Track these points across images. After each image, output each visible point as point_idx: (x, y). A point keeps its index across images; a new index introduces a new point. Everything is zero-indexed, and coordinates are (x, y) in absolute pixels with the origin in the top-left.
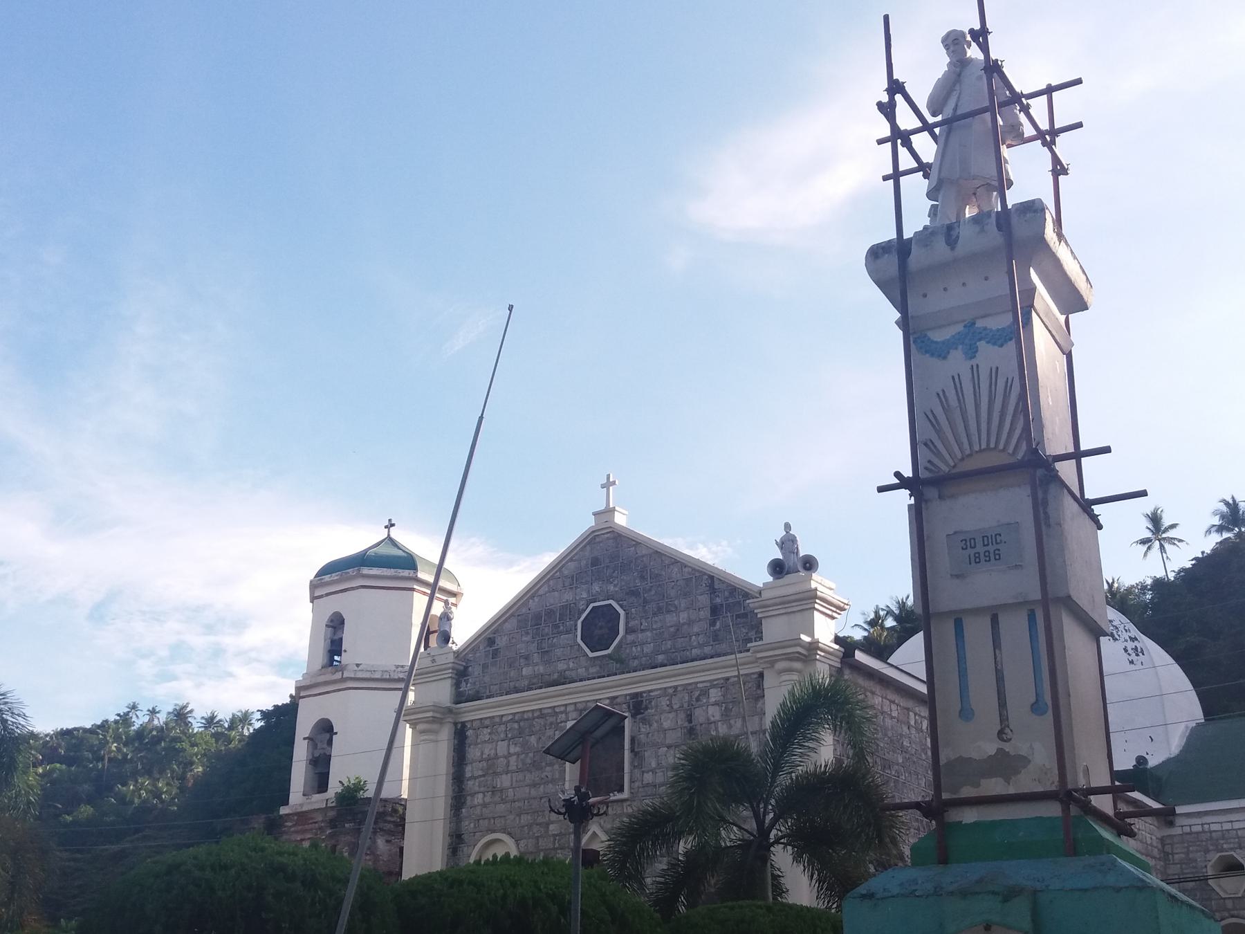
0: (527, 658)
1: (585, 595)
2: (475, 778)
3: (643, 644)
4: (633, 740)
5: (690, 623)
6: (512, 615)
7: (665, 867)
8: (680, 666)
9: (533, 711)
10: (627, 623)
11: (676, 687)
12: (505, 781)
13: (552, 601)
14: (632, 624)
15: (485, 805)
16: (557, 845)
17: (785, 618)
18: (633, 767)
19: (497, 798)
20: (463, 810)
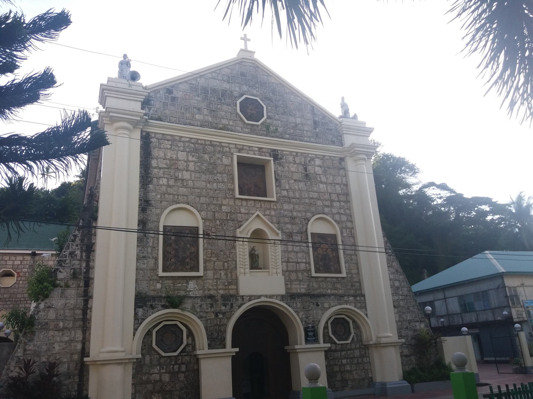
0: (199, 109)
2: (160, 168)
6: (186, 82)
9: (205, 140)
11: (297, 153)
12: (186, 175)
14: (269, 114)
16: (229, 218)
19: (179, 184)
20: (150, 186)
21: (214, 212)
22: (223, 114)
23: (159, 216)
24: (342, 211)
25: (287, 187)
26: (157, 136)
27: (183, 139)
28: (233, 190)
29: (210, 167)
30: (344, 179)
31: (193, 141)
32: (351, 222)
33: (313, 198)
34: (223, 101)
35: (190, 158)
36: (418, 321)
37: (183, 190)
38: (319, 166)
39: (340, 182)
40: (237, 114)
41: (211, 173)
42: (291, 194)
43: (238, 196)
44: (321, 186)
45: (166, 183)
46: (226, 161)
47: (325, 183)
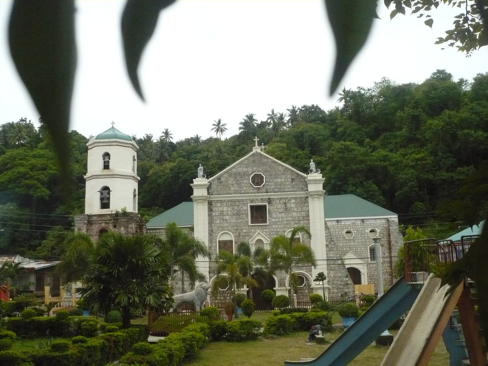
0: (233, 185)
1: (251, 170)
2: (216, 216)
3: (271, 186)
4: (269, 210)
5: (285, 182)
7: (49, 232)
8: (282, 193)
10: (266, 179)
11: (281, 198)
12: (227, 218)
13: (240, 170)
15: (220, 223)
16: (246, 235)
17: (315, 184)
18: (269, 217)
19: (224, 222)
21: (239, 233)
22: (243, 185)
23: (217, 236)
25: (275, 217)
26: (215, 201)
27: (226, 201)
28: (248, 222)
29: (238, 212)
30: (307, 208)
31: (230, 201)
33: (289, 221)
34: (244, 178)
35: (229, 209)
36: (344, 277)
37: (226, 225)
38: (294, 203)
40: (250, 183)
41: (238, 215)
42: (277, 220)
43: (250, 224)
44: (294, 213)
45: (219, 222)
46: (245, 208)
47: (297, 212)
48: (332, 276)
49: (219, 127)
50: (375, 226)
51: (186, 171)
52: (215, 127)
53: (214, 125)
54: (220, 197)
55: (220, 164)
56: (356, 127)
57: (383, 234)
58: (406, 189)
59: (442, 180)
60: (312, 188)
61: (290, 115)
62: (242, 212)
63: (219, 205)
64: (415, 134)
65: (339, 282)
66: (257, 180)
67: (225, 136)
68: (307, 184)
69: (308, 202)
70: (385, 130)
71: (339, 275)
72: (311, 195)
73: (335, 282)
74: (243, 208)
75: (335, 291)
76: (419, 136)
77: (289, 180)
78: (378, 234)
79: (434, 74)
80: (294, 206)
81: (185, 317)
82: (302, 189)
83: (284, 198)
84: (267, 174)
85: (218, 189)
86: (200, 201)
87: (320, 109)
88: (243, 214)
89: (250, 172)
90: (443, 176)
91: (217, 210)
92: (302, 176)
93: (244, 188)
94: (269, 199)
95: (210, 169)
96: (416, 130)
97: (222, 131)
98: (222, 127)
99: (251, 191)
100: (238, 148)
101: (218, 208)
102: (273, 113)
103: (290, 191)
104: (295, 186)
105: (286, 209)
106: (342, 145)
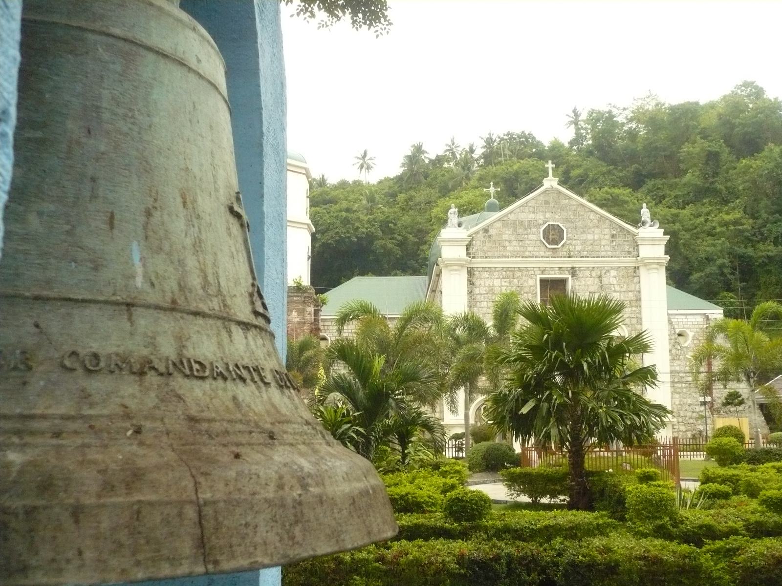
0: (510, 242)
1: (542, 217)
3: (575, 246)
5: (600, 240)
8: (596, 259)
13: (522, 217)
22: (529, 242)
24: (633, 315)
26: (479, 269)
30: (638, 286)
32: (641, 324)
35: (503, 284)
39: (633, 289)
40: (541, 240)
46: (531, 282)
47: (618, 292)
48: (677, 403)
49: (365, 164)
50: (686, 326)
51: (328, 230)
52: (359, 160)
53: (358, 158)
54: (489, 262)
55: (381, 222)
56: (605, 168)
57: (698, 339)
58: (712, 269)
59: (769, 257)
60: (646, 251)
61: (484, 147)
62: (526, 290)
63: (485, 275)
64: (713, 183)
65: (689, 414)
66: (553, 235)
67: (372, 178)
68: (637, 246)
69: (639, 276)
70: (652, 176)
71: (689, 401)
72: (645, 265)
73: (682, 414)
74: (527, 283)
75: (682, 428)
76: (719, 186)
77: (607, 237)
78: (690, 339)
79: (737, 87)
80: (615, 283)
81: (602, 460)
82: (629, 253)
83: (598, 267)
84: (568, 224)
85: (485, 248)
86: (456, 267)
87: (534, 138)
88: (527, 293)
89: (540, 222)
90: (768, 251)
91: (482, 284)
92: (628, 232)
93: (530, 249)
94: (573, 268)
95: (367, 228)
96: (714, 177)
97: (369, 168)
98: (370, 162)
99: (542, 254)
100: (401, 197)
101: (483, 282)
102: (453, 144)
103: (608, 257)
104: (616, 247)
105: (601, 287)
106: (607, 193)
